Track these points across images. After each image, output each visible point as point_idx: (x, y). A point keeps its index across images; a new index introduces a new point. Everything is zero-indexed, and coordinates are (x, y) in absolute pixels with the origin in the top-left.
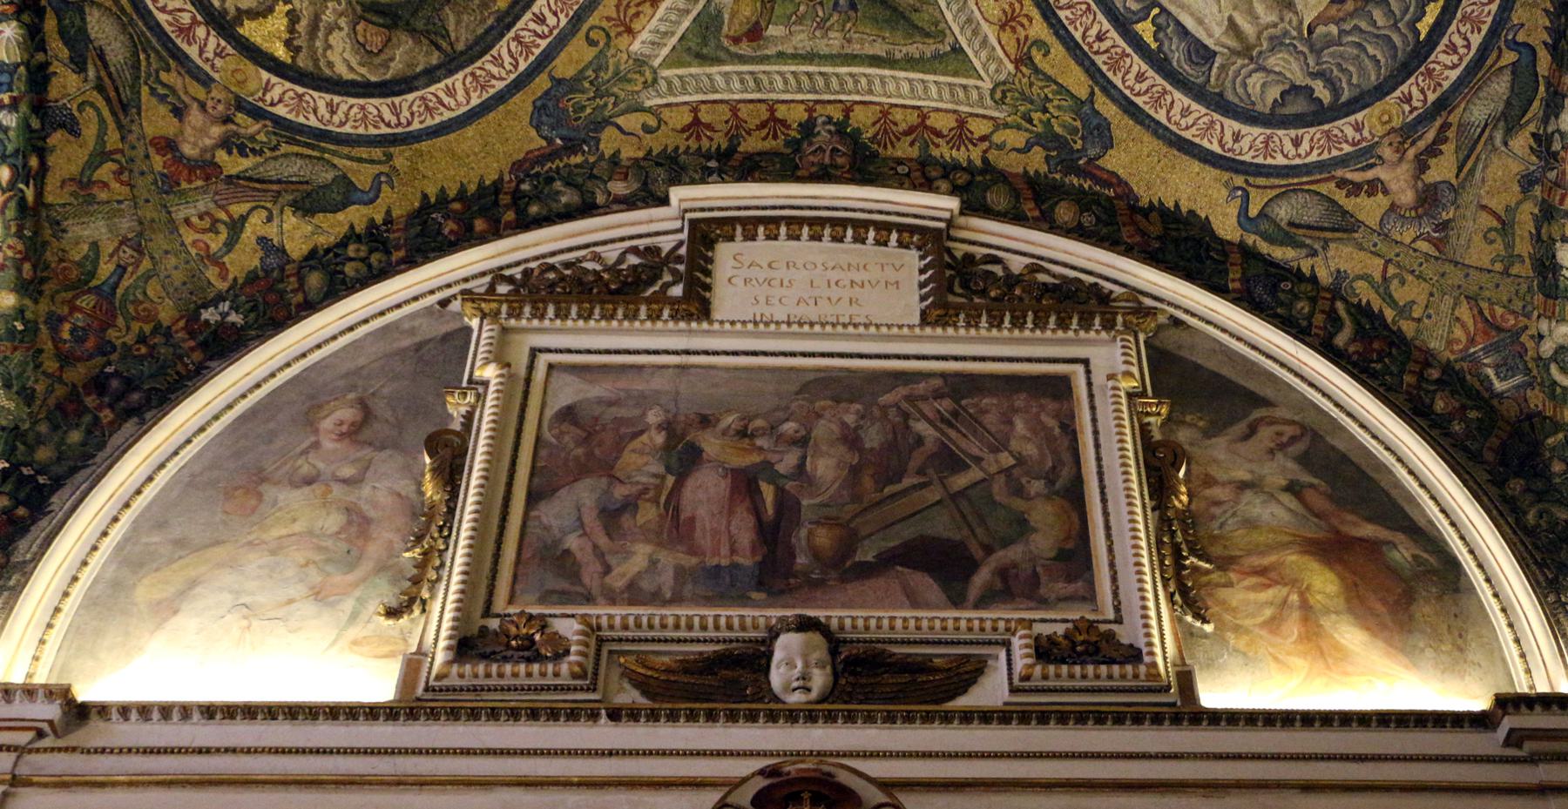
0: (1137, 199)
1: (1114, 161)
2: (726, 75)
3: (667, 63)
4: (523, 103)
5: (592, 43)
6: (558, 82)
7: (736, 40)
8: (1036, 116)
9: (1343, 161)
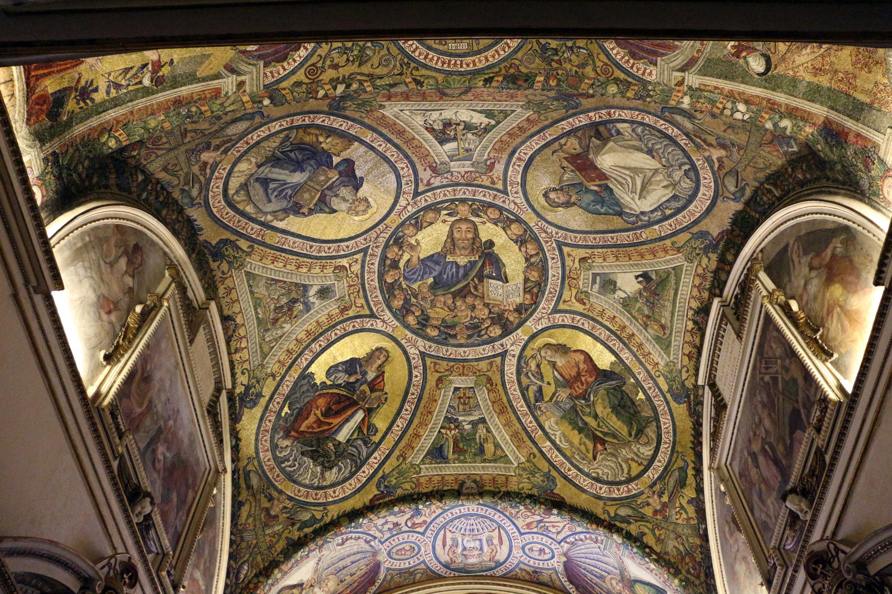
0: (728, 230)
1: (715, 232)
2: (675, 341)
3: (669, 356)
4: (673, 404)
5: (659, 376)
6: (669, 391)
7: (665, 333)
8: (697, 251)
9: (712, 168)
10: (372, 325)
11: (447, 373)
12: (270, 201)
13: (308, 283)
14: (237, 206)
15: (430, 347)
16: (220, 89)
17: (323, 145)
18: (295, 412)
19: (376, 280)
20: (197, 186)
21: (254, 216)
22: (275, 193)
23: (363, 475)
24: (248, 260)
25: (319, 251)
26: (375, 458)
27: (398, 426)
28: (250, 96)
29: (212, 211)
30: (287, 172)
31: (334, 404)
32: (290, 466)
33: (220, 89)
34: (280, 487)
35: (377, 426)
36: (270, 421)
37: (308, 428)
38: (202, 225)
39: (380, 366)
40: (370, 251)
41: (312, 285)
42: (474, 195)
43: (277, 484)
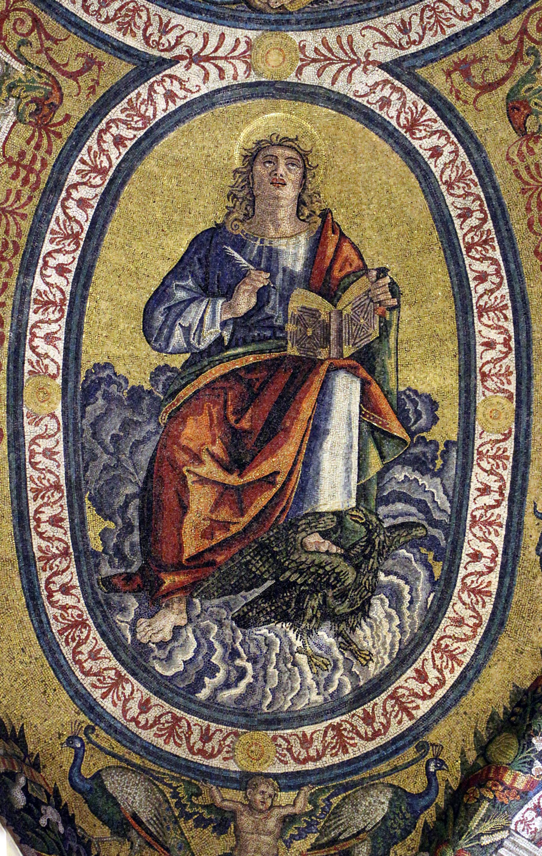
10: (170, 96)
11: (521, 70)
15: (404, 28)
18: (133, 513)
23: (479, 566)
26: (485, 490)
27: (490, 345)
31: (240, 413)
32: (227, 685)
34: (233, 767)
35: (422, 388)
36: (66, 590)
37: (207, 534)
39: (300, 202)
43: (216, 762)
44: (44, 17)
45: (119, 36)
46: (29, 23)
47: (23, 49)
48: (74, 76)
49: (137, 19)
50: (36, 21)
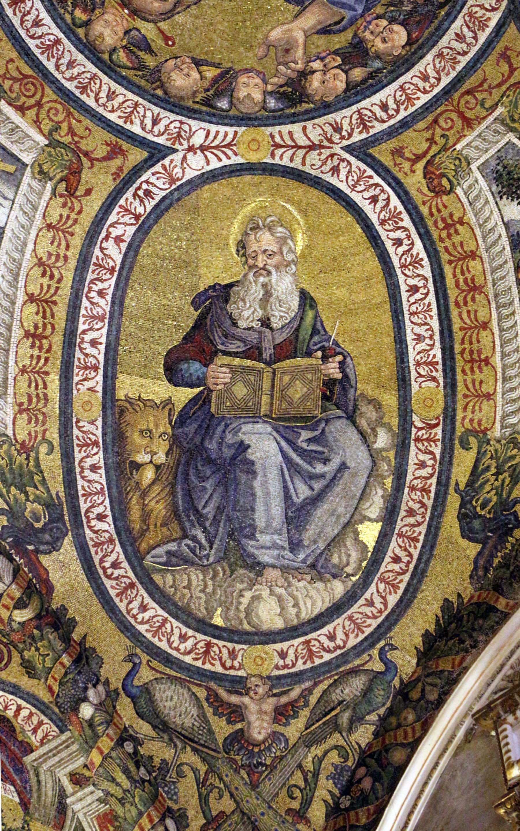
12: (343, 467)
13: (505, 241)
14: (371, 544)
16: (98, 818)
17: (161, 458)
19: (419, 67)
20: (336, 696)
21: (389, 482)
22: (320, 468)
24: (497, 432)
25: (417, 262)
28: (88, 752)
29: (397, 605)
30: (257, 484)
33: (98, 818)
38: (436, 608)
40: (357, 137)
41: (507, 225)
42: (58, 42)
44: (467, 85)
45: (488, 31)
46: (468, 98)
47: (487, 105)
48: (512, 70)
49: (477, 15)
50: (468, 92)
